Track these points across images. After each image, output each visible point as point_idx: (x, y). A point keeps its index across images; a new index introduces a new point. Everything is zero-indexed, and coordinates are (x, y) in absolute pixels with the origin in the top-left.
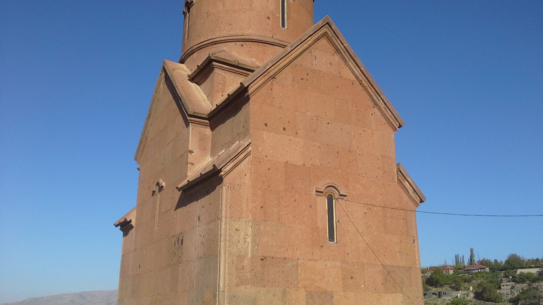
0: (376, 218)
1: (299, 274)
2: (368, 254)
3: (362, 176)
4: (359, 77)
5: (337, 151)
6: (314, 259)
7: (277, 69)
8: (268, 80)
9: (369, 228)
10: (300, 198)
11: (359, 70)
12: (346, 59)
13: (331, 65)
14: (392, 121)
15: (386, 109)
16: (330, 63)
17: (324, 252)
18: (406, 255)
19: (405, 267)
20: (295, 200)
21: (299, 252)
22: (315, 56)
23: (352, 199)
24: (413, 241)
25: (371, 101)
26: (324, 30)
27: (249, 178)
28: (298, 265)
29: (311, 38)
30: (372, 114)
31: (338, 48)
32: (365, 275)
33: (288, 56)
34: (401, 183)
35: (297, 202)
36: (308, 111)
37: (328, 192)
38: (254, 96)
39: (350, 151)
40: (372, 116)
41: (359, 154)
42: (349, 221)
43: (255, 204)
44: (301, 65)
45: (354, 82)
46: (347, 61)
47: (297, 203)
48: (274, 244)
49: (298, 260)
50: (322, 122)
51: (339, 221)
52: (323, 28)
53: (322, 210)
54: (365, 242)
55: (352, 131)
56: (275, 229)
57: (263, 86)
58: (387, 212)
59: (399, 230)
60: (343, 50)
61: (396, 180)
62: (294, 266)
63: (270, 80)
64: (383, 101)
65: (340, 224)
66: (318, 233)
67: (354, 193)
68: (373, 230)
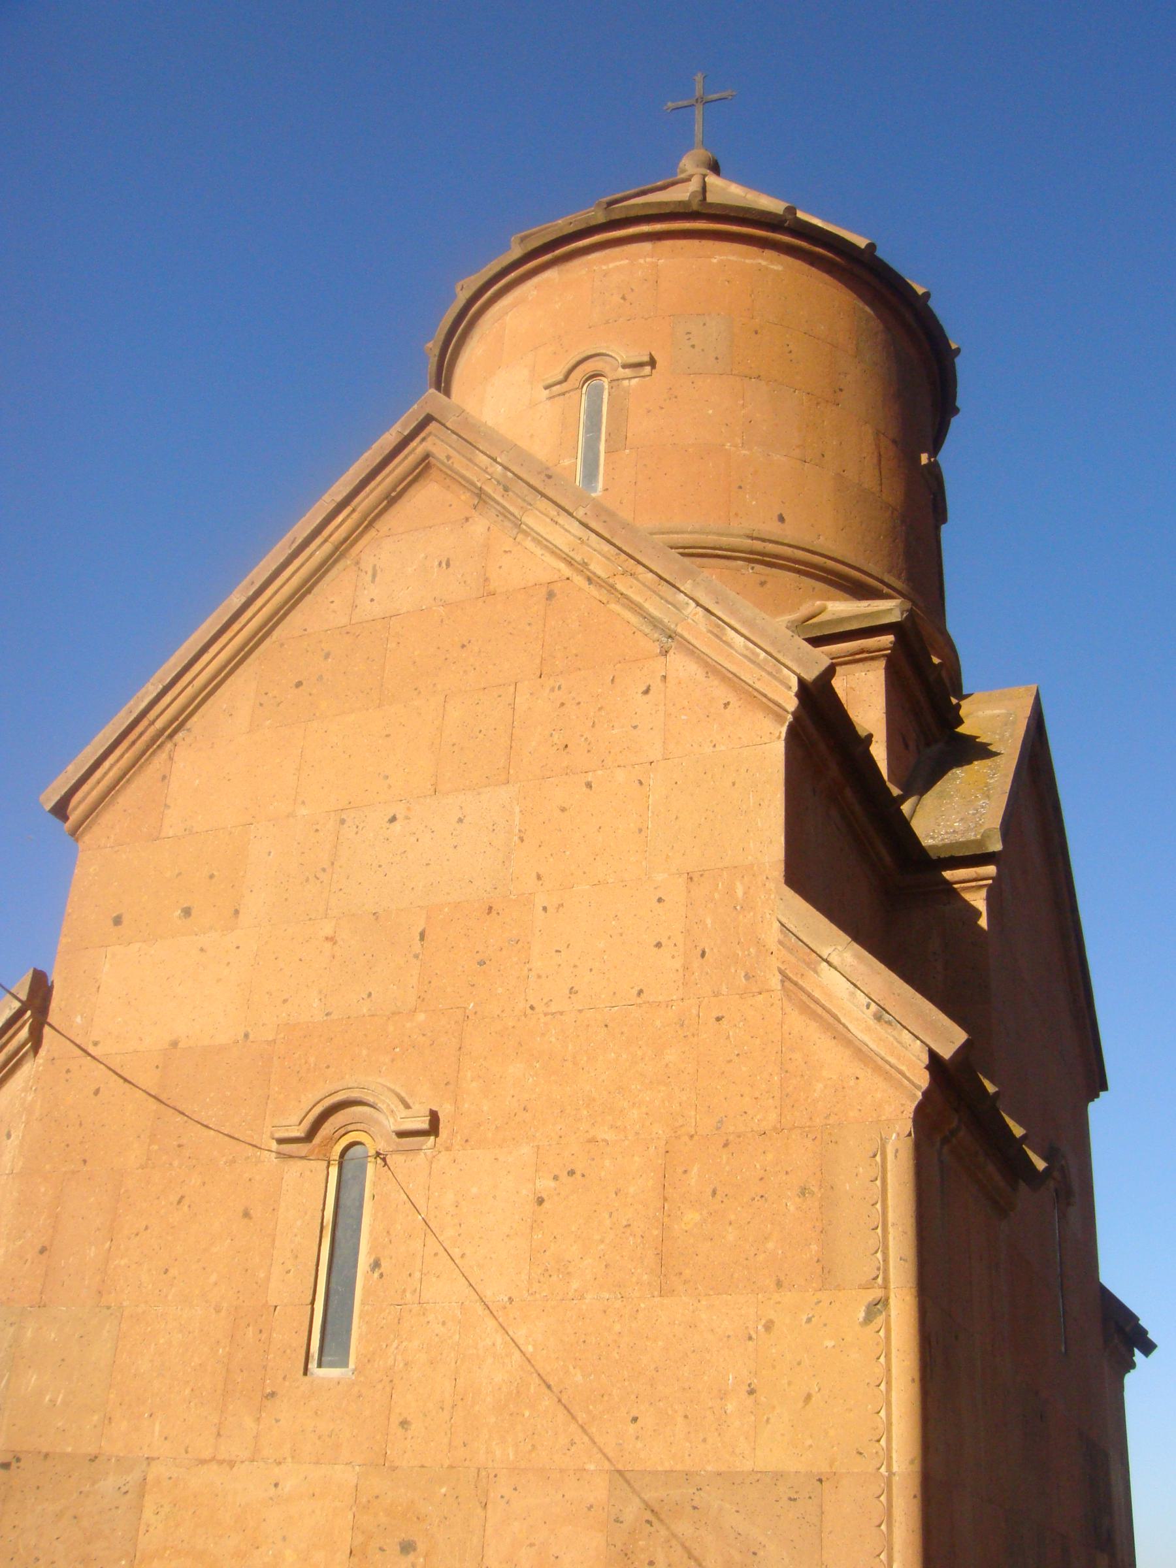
0: (607, 1216)
1: (143, 1528)
2: (527, 1414)
3: (545, 1015)
4: (571, 554)
5: (420, 930)
6: (219, 1457)
7: (190, 691)
8: (151, 750)
9: (554, 1278)
10: (204, 1184)
11: (576, 528)
12: (512, 509)
13: (448, 565)
14: (749, 674)
15: (717, 636)
16: (440, 564)
17: (277, 1421)
18: (801, 1404)
19: (778, 1476)
20: (182, 1197)
21: (157, 1428)
22: (374, 566)
23: (467, 1141)
24: (861, 1315)
25: (647, 631)
26: (417, 448)
27: (17, 1142)
28: (148, 1487)
29: (354, 510)
30: (647, 692)
31: (476, 486)
32: (489, 1531)
33: (236, 627)
34: (796, 984)
35: (189, 1206)
36: (303, 803)
37: (342, 1131)
38: (95, 829)
39: (490, 908)
40: (646, 698)
41: (545, 909)
42: (436, 1254)
43: (23, 1240)
44: (305, 630)
45: (556, 588)
46: (516, 514)
47: (186, 1208)
48: (61, 1396)
49: (149, 1464)
50: (360, 828)
51: (376, 1265)
52: (414, 444)
53: (299, 1223)
54: (517, 1355)
55: (517, 809)
56: (76, 1336)
57: (128, 780)
58: (685, 1172)
59: (761, 1257)
60: (499, 483)
61: (775, 981)
62: (126, 1492)
63: (159, 747)
64: (698, 604)
65: (381, 1275)
66: (261, 1331)
67: (485, 1108)
68: (575, 1285)
